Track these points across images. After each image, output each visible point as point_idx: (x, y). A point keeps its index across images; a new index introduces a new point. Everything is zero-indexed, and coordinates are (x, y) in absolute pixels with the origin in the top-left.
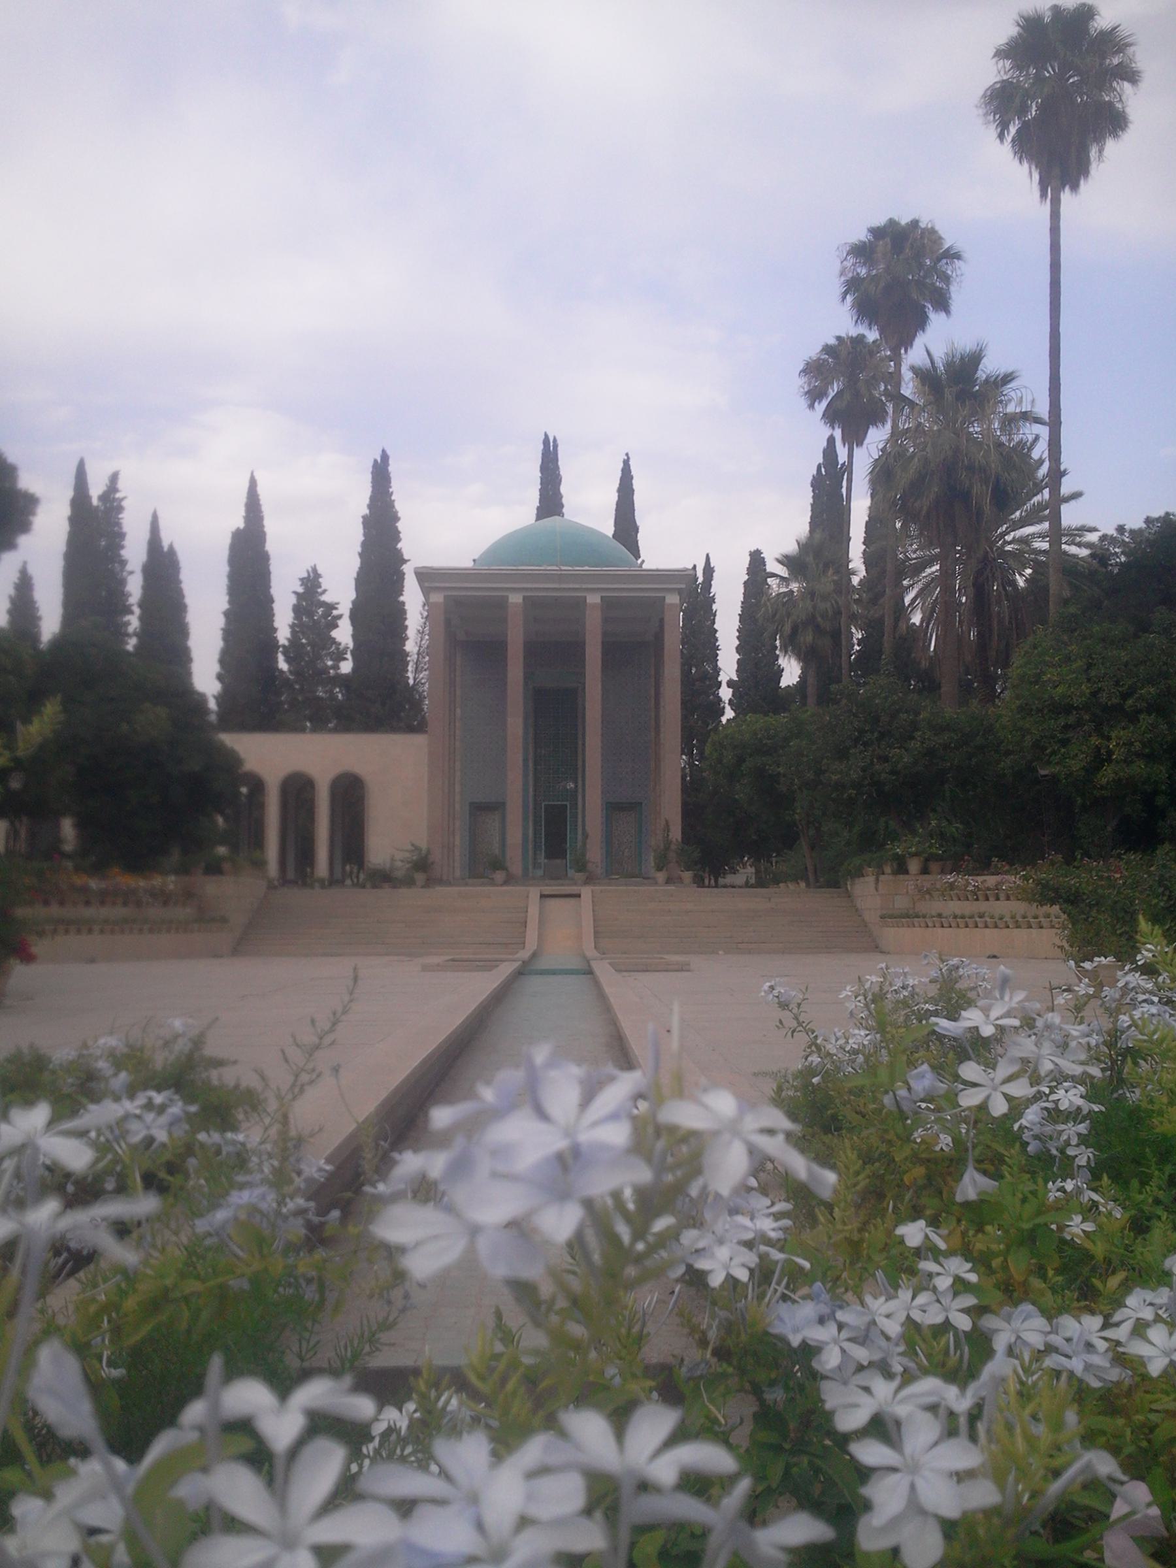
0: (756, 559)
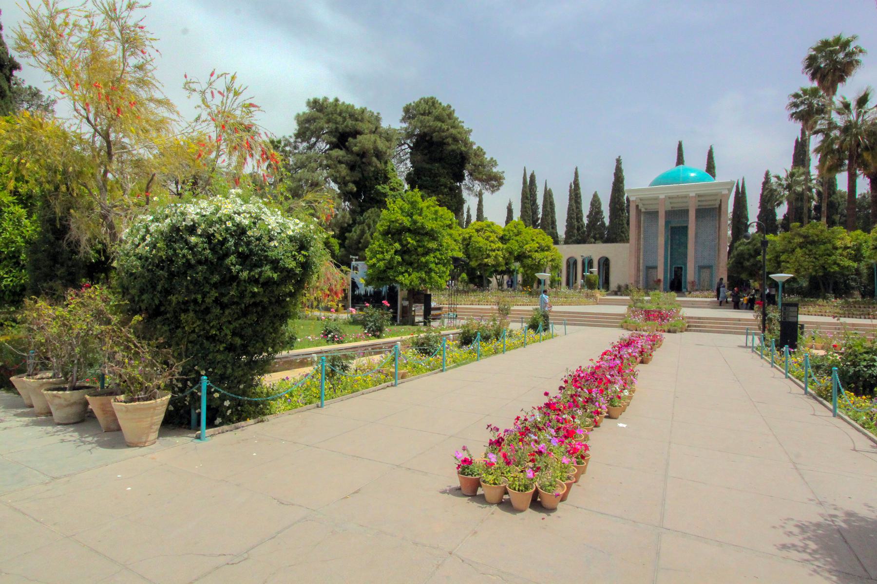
0: (767, 174)
